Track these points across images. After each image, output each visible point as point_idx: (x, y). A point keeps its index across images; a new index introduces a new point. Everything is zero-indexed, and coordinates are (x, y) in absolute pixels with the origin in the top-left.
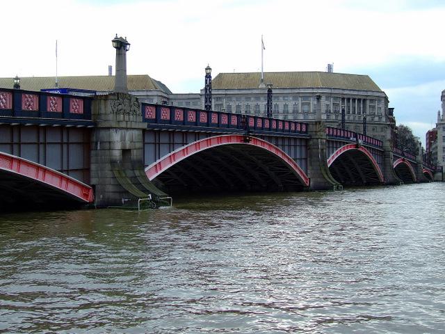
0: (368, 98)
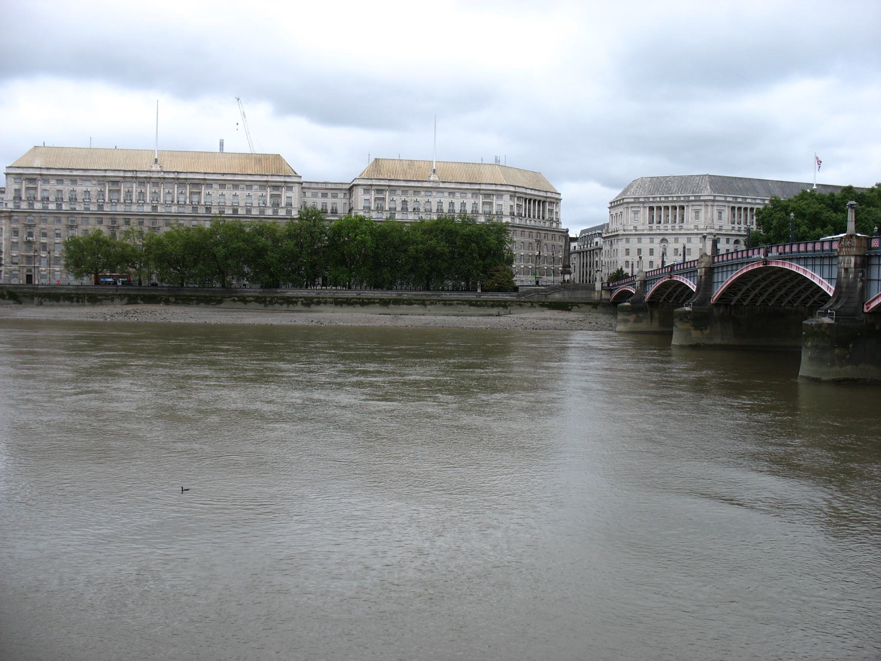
0: (548, 200)
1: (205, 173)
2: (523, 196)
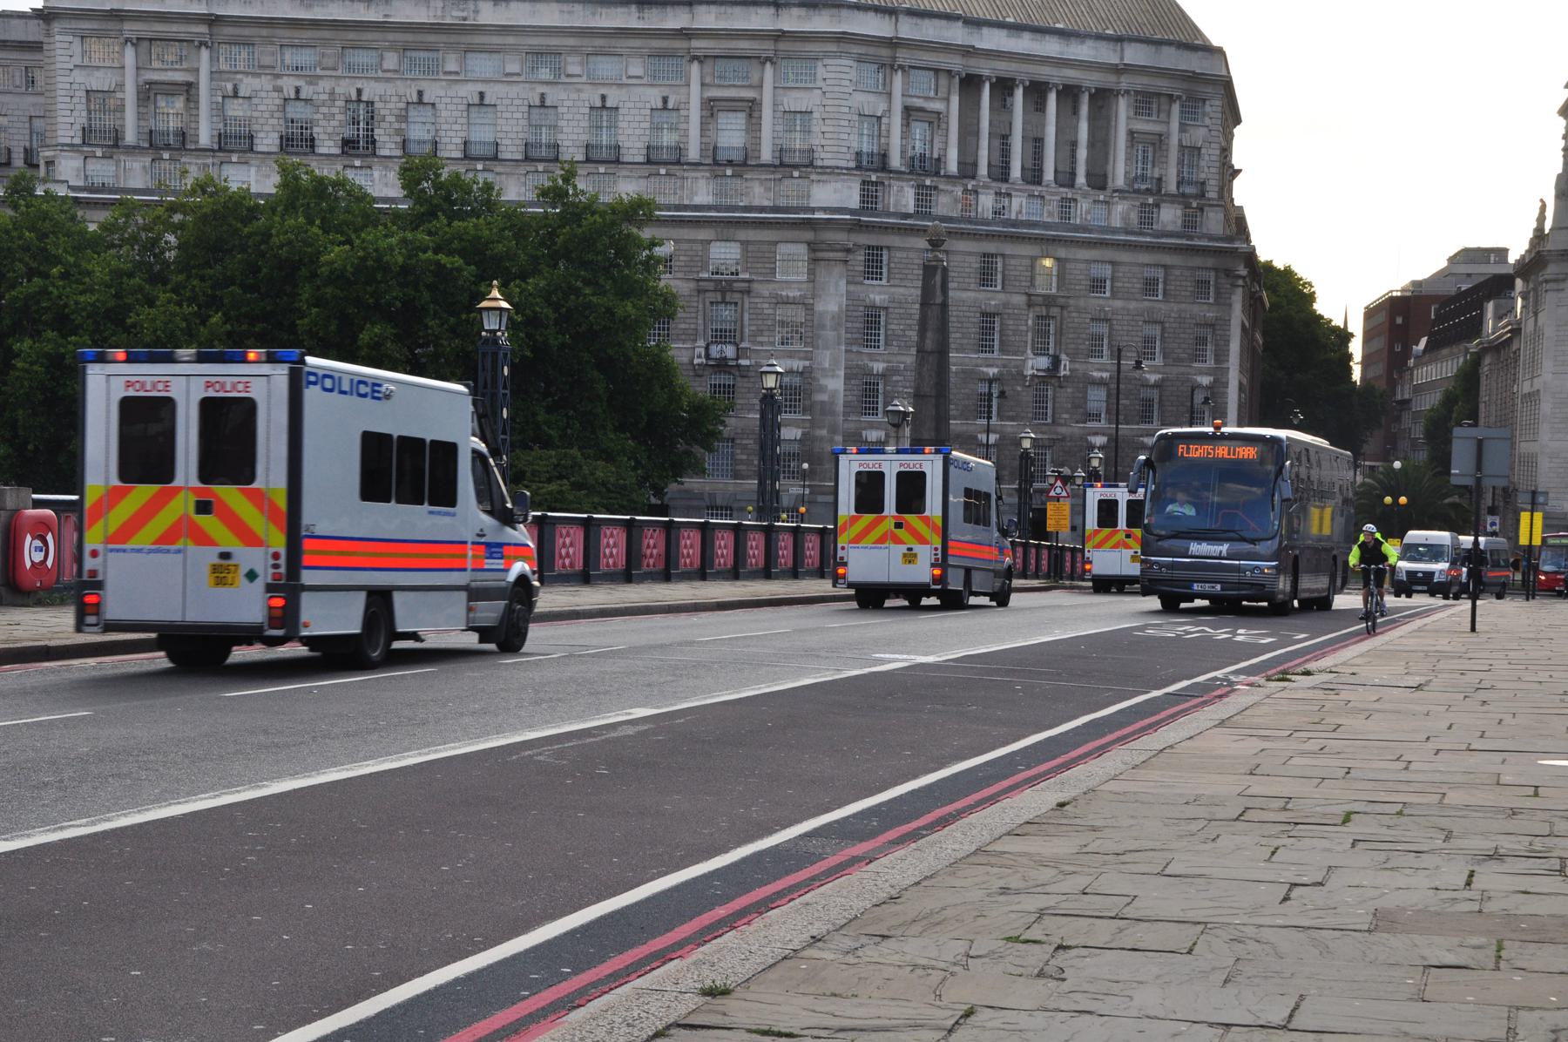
0: (1125, 82)
2: (956, 63)
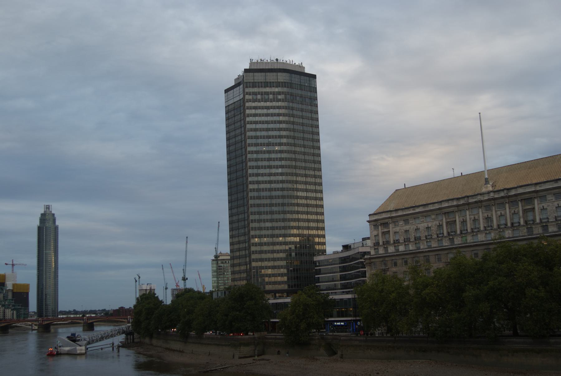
1: (536, 184)
